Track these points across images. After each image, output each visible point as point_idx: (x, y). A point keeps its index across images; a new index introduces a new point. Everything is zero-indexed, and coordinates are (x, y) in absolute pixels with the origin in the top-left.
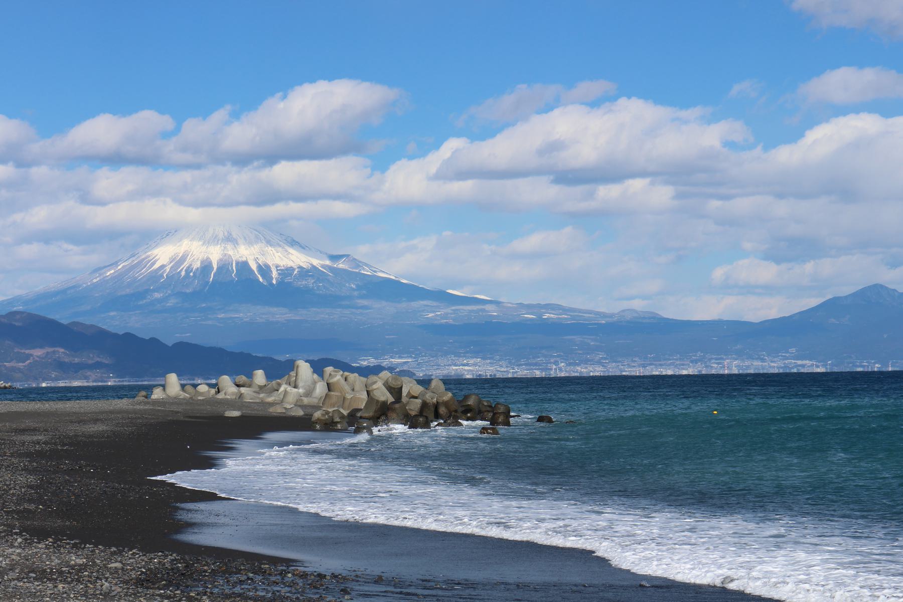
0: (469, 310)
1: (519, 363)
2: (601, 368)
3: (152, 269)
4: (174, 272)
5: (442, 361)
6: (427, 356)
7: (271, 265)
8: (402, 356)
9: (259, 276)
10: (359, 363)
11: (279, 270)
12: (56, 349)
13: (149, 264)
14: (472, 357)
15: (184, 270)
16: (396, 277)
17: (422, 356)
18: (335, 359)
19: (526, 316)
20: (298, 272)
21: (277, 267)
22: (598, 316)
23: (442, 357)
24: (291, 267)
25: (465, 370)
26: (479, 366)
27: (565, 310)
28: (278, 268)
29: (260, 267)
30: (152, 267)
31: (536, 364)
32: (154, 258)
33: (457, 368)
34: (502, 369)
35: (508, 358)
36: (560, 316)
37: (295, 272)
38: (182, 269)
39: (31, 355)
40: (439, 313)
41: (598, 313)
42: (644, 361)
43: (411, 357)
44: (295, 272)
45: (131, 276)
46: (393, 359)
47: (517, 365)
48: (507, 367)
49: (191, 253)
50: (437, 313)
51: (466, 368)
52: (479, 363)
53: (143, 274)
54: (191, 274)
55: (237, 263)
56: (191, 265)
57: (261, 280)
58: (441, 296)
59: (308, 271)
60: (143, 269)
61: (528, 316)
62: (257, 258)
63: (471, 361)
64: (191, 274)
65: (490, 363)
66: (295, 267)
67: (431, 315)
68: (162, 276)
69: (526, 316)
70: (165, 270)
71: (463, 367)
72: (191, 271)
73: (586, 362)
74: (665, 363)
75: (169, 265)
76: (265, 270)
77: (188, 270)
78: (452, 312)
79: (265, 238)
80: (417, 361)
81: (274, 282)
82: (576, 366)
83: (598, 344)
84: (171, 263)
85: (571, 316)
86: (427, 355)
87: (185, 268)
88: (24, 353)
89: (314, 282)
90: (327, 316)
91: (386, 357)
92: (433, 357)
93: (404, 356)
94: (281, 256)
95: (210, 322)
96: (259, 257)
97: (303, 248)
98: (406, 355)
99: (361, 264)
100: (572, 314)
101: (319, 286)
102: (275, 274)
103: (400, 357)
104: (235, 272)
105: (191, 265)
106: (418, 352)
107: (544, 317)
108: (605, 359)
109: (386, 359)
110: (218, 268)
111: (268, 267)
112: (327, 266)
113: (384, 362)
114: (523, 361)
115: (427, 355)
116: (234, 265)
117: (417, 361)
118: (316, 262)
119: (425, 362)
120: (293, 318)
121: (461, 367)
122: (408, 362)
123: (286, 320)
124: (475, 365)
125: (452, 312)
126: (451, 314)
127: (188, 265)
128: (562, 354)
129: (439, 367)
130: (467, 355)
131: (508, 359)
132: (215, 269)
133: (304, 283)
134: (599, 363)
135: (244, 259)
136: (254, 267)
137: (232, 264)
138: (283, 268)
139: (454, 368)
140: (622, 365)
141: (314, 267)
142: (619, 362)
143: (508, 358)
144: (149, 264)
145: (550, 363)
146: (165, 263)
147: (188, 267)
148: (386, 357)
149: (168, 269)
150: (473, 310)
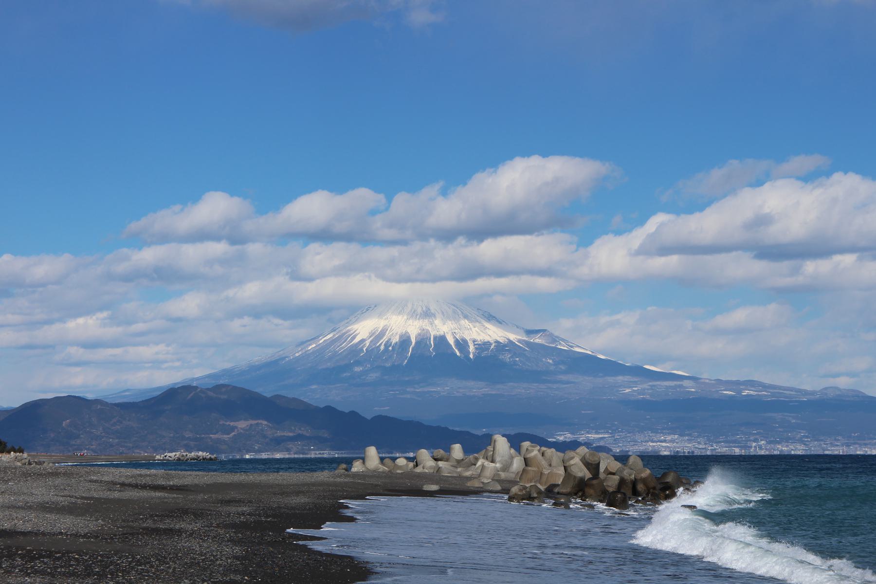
0: (666, 386)
1: (718, 440)
2: (802, 447)
3: (353, 343)
4: (373, 347)
5: (639, 437)
6: (624, 432)
7: (468, 340)
8: (599, 431)
9: (457, 351)
10: (555, 438)
11: (477, 344)
12: (260, 421)
13: (350, 338)
14: (670, 434)
15: (383, 344)
16: (593, 352)
17: (619, 432)
18: (531, 434)
19: (725, 392)
20: (494, 346)
21: (474, 341)
22: (799, 394)
24: (488, 342)
25: (663, 446)
26: (677, 443)
27: (765, 387)
28: (476, 343)
29: (457, 342)
30: (351, 342)
31: (735, 442)
32: (354, 332)
33: (654, 444)
34: (701, 446)
35: (707, 434)
36: (760, 393)
37: (492, 347)
39: (236, 427)
41: (799, 391)
42: (848, 440)
43: (608, 432)
44: (492, 347)
47: (716, 442)
48: (705, 444)
49: (390, 328)
51: (664, 444)
52: (676, 439)
54: (390, 348)
55: (435, 338)
56: (390, 339)
57: (458, 354)
58: (639, 371)
59: (505, 346)
61: (727, 392)
62: (455, 333)
63: (669, 438)
64: (390, 348)
65: (688, 440)
67: (627, 391)
68: (362, 350)
69: (725, 392)
70: (365, 344)
71: (661, 444)
73: (787, 440)
74: (870, 443)
76: (462, 344)
78: (649, 387)
79: (462, 313)
80: (614, 437)
81: (471, 356)
82: (777, 445)
83: (799, 421)
84: (370, 337)
85: (771, 392)
86: (624, 431)
87: (384, 342)
88: (229, 425)
89: (511, 357)
90: (523, 391)
92: (629, 433)
93: (601, 431)
95: (408, 396)
97: (500, 323)
98: (603, 431)
99: (558, 340)
100: (771, 391)
101: (516, 360)
102: (472, 348)
103: (597, 433)
104: (433, 346)
105: (390, 339)
107: (743, 394)
108: (807, 437)
109: (582, 434)
110: (416, 343)
111: (465, 341)
112: (524, 340)
113: (581, 437)
114: (722, 439)
115: (624, 431)
116: (432, 339)
117: (614, 437)
118: (513, 337)
119: (622, 438)
120: (490, 393)
121: (658, 443)
122: (605, 438)
123: (483, 394)
124: (672, 441)
125: (649, 387)
126: (648, 389)
127: (387, 339)
128: (762, 431)
129: (636, 443)
130: (664, 431)
131: (706, 436)
134: (801, 441)
135: (442, 333)
136: (451, 341)
137: (430, 339)
138: (480, 343)
139: (651, 444)
140: (825, 444)
141: (510, 341)
142: (822, 440)
143: (707, 434)
144: (350, 338)
145: (750, 441)
147: (387, 342)
149: (367, 343)
150: (671, 386)
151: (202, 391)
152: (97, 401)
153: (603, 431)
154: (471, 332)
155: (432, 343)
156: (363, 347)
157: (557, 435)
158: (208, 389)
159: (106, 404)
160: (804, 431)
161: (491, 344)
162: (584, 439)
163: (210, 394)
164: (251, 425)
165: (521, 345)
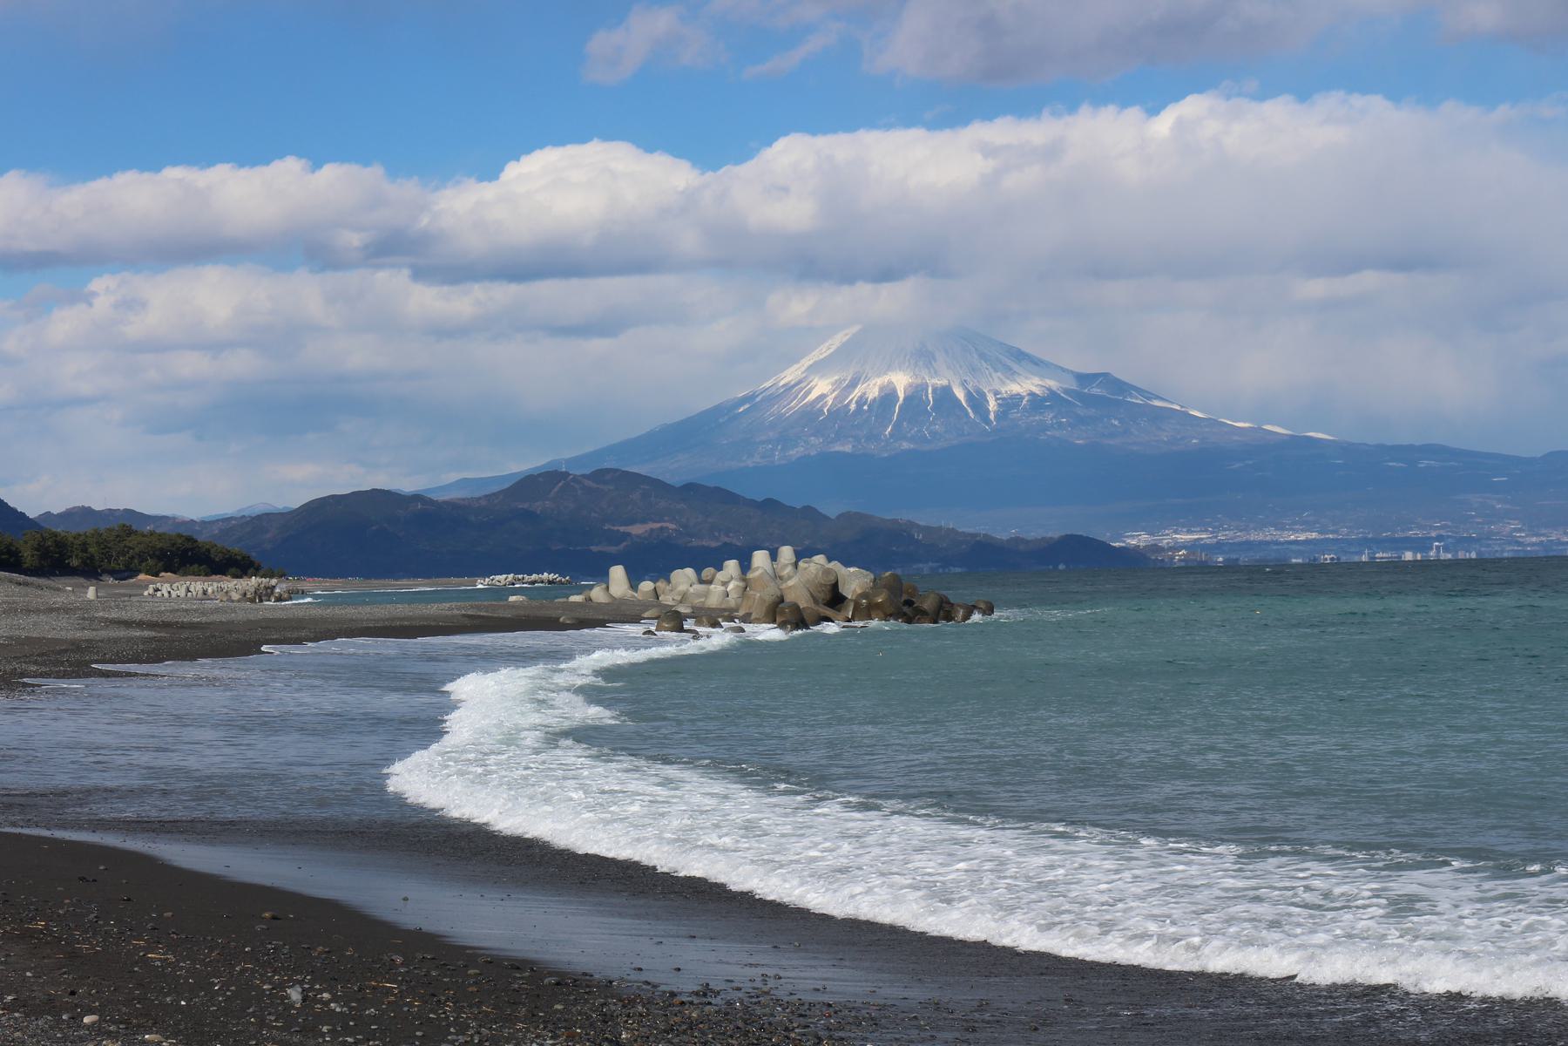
6: (1233, 530)
7: (986, 391)
9: (970, 411)
10: (1124, 542)
12: (664, 525)
13: (802, 393)
15: (854, 402)
16: (1182, 407)
17: (1225, 530)
18: (1085, 535)
19: (1391, 464)
21: (995, 394)
23: (1256, 531)
24: (1018, 394)
28: (998, 396)
32: (808, 384)
35: (1361, 530)
37: (1024, 402)
38: (852, 400)
39: (629, 534)
40: (1250, 462)
43: (1206, 531)
45: (776, 412)
46: (1178, 534)
49: (864, 376)
50: (1247, 462)
53: (791, 409)
54: (866, 407)
55: (934, 390)
56: (865, 394)
59: (1044, 399)
60: (792, 402)
62: (965, 381)
64: (866, 407)
66: (1025, 394)
67: (1237, 465)
68: (821, 410)
69: (1391, 464)
72: (865, 403)
75: (831, 394)
77: (861, 401)
79: (976, 349)
83: (1508, 506)
84: (834, 391)
87: (855, 399)
88: (618, 531)
89: (1055, 417)
91: (1167, 532)
94: (1002, 377)
96: (967, 378)
97: (1036, 364)
98: (1199, 529)
101: (1061, 422)
102: (992, 405)
103: (1189, 532)
105: (865, 394)
106: (1217, 524)
108: (1520, 530)
109: (1168, 535)
110: (904, 400)
117: (1216, 537)
127: (859, 394)
128: (1450, 523)
132: (901, 399)
133: (1037, 418)
136: (960, 394)
143: (1361, 530)
144: (802, 393)
146: (825, 392)
147: (861, 397)
148: (1167, 532)
149: (830, 400)
151: (576, 479)
152: (416, 497)
153: (1199, 529)
154: (991, 380)
155: (930, 396)
156: (823, 406)
157: (1127, 537)
158: (584, 476)
159: (431, 502)
160: (1516, 522)
161: (1022, 398)
162: (1168, 543)
163: (588, 483)
164: (652, 530)
165: (1070, 399)
